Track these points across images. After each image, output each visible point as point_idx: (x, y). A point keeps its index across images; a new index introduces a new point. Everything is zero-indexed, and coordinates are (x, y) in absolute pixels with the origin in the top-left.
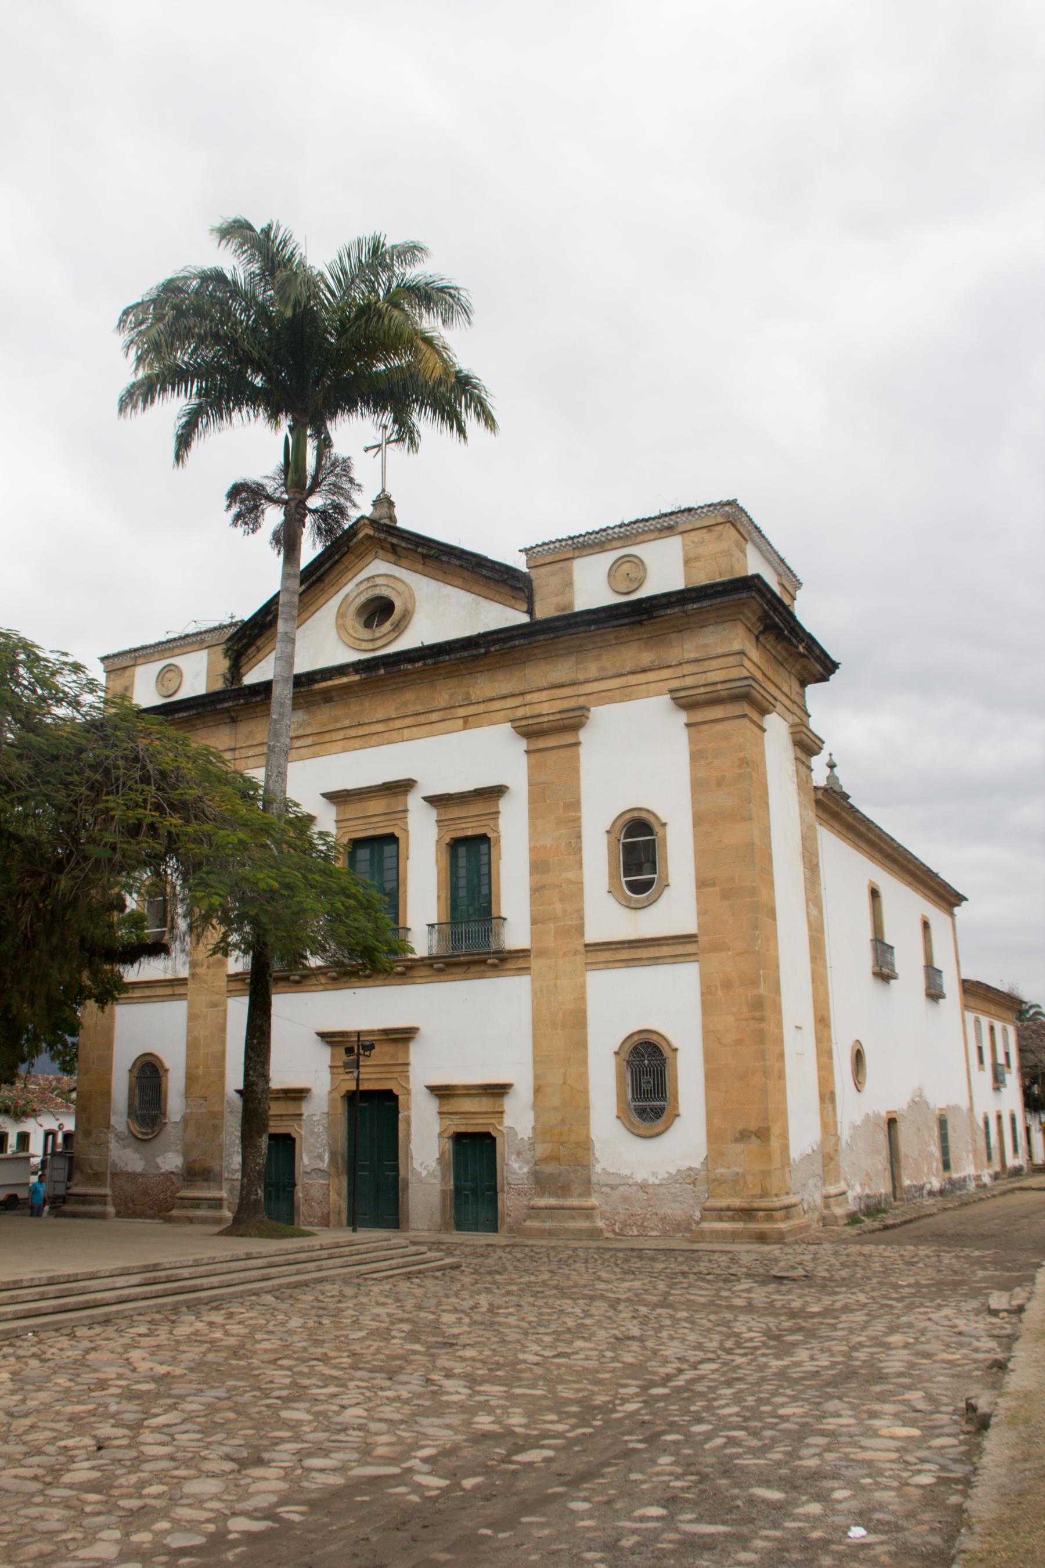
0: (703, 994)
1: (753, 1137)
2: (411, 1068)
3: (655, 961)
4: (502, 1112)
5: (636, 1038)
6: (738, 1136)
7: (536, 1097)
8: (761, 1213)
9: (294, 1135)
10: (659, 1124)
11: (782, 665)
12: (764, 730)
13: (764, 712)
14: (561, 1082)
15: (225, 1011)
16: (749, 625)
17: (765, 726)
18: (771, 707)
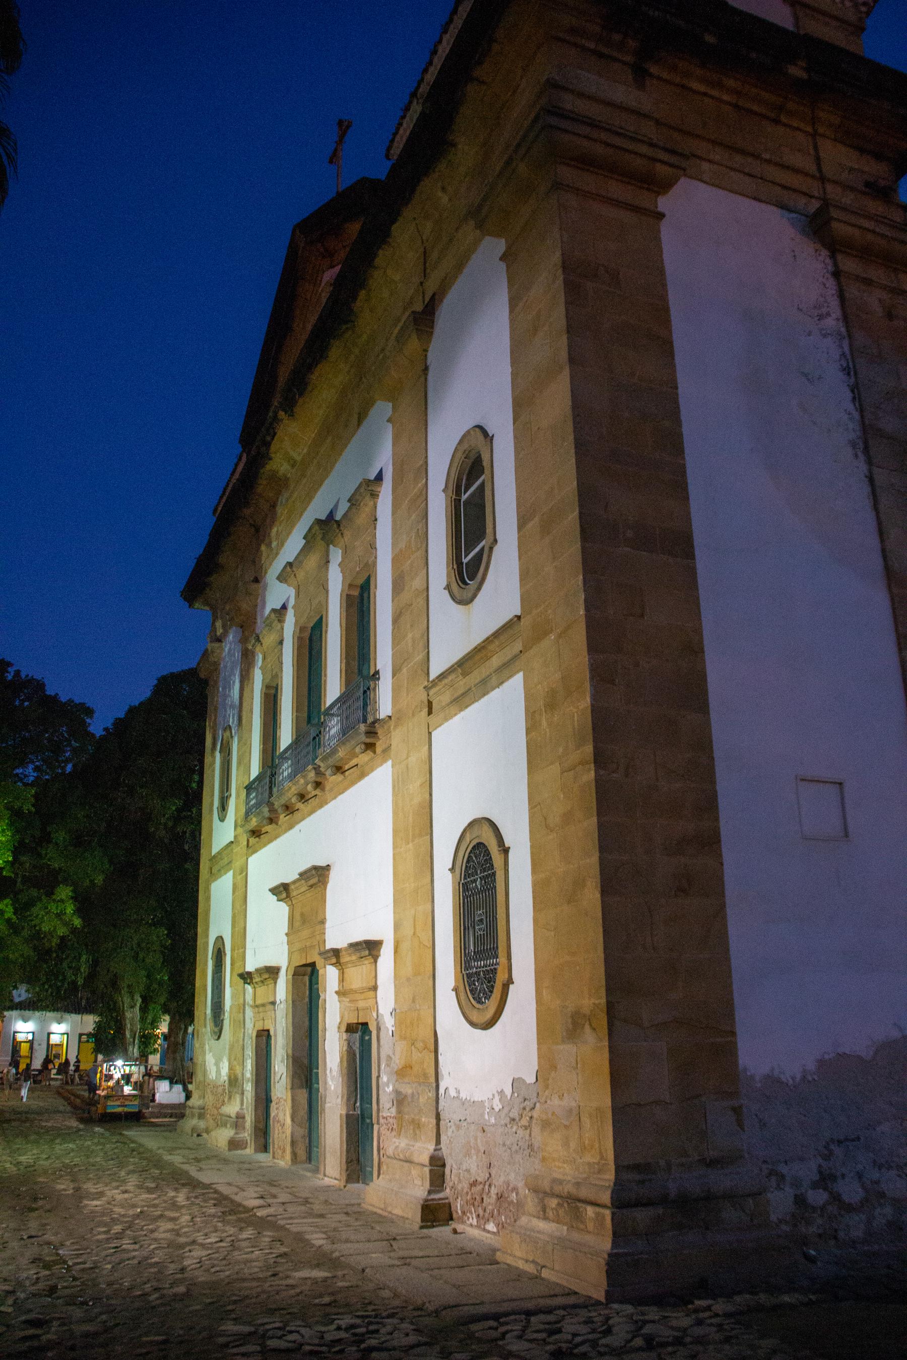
0: (528, 731)
1: (587, 1026)
2: (328, 925)
3: (484, 688)
4: (375, 988)
5: (468, 838)
6: (571, 1026)
7: (395, 962)
8: (590, 1211)
9: (272, 1033)
10: (492, 1005)
11: (776, 122)
12: (661, 216)
13: (664, 186)
14: (412, 933)
15: (247, 874)
16: (592, 45)
17: (660, 209)
18: (660, 168)
